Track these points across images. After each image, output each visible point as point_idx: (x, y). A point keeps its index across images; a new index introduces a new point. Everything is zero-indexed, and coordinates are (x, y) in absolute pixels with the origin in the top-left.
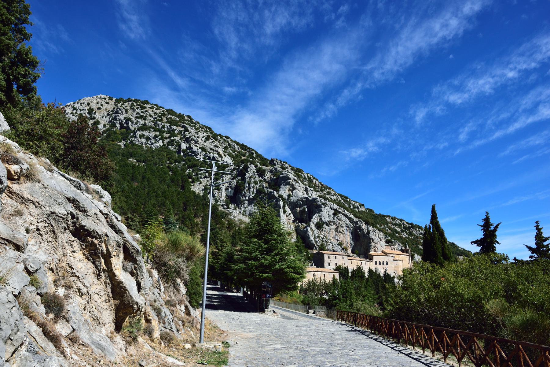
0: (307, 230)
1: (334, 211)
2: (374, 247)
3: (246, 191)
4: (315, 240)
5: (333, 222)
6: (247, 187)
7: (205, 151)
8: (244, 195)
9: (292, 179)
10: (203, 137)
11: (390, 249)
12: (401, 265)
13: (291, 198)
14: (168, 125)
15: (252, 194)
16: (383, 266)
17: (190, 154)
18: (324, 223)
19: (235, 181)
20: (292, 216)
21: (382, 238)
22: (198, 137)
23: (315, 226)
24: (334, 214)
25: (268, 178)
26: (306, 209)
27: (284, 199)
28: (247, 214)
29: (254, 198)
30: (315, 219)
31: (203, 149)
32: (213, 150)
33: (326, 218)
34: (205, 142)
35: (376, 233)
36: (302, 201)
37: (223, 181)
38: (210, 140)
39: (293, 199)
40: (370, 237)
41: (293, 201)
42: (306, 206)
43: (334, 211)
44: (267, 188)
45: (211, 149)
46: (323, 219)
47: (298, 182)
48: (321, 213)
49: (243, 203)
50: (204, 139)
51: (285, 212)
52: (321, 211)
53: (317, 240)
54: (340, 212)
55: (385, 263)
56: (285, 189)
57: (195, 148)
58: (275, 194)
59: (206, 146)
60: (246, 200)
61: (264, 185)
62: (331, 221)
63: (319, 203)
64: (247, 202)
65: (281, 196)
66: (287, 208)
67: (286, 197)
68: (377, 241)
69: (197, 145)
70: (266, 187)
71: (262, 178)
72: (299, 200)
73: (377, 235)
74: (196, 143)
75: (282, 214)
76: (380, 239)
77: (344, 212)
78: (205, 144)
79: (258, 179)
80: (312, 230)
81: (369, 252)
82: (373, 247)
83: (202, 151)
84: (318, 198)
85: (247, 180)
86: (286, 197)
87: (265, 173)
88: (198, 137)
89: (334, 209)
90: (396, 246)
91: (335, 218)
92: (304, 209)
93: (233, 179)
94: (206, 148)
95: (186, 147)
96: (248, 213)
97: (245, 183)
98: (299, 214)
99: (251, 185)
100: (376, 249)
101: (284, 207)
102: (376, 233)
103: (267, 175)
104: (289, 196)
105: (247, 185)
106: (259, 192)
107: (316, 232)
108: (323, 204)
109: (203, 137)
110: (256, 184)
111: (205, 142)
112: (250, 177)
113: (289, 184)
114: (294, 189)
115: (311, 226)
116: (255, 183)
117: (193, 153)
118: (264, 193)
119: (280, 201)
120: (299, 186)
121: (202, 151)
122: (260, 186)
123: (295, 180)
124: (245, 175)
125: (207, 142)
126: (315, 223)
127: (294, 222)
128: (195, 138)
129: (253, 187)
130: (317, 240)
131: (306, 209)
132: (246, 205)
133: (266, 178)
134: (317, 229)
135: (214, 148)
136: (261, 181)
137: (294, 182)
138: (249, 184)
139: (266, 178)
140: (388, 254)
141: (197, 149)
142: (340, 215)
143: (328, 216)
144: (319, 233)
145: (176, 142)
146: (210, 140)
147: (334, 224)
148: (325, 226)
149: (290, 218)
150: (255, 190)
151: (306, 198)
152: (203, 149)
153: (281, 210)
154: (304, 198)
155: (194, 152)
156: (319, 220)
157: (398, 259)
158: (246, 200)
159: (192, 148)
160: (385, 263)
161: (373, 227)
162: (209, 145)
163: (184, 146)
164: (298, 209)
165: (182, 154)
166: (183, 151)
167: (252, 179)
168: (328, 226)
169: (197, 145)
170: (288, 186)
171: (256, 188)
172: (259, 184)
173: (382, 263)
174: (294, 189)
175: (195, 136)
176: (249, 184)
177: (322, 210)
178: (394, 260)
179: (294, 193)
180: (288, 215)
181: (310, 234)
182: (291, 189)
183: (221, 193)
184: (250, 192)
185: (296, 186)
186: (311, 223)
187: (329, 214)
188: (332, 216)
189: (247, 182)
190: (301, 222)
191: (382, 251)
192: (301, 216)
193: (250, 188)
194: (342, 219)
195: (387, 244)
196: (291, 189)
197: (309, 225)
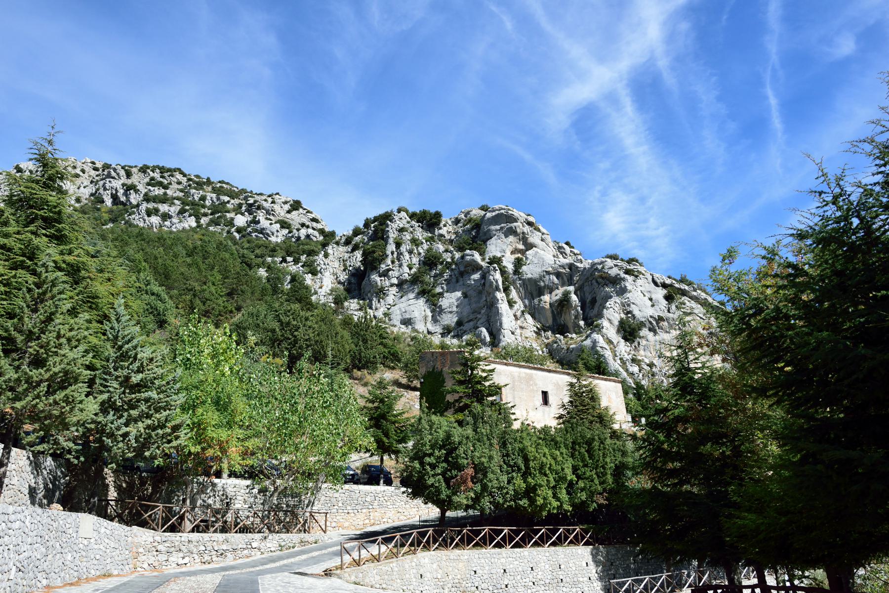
0: (595, 342)
1: (665, 292)
3: (389, 262)
4: (627, 371)
5: (667, 320)
6: (392, 253)
7: (288, 228)
8: (385, 274)
9: (522, 220)
10: (285, 203)
13: (524, 268)
14: (214, 196)
15: (406, 270)
17: (253, 235)
18: (642, 325)
19: (358, 255)
20: (528, 317)
22: (273, 202)
23: (618, 331)
24: (669, 298)
25: (449, 232)
26: (574, 298)
27: (503, 272)
28: (398, 323)
29: (415, 280)
30: (613, 313)
31: (284, 224)
32: (308, 227)
33: (643, 310)
34: (289, 212)
36: (558, 275)
37: (326, 255)
38: (301, 210)
39: (530, 271)
41: (529, 276)
42: (571, 288)
43: (665, 292)
44: (451, 252)
45: (303, 225)
46: (636, 312)
47: (539, 230)
48: (628, 295)
49: (381, 293)
50: (287, 207)
51: (511, 303)
52: (623, 291)
53: (635, 369)
54: (684, 293)
56: (504, 247)
57: (264, 223)
58: (477, 257)
59: (292, 220)
60: (392, 285)
61: (441, 247)
62: (661, 319)
63: (614, 272)
64: (394, 290)
65: (496, 261)
66: (514, 294)
67: (508, 263)
69: (271, 217)
70: (446, 251)
71: (433, 232)
72: (548, 273)
74: (268, 212)
75: (503, 307)
77: (695, 293)
78: (288, 216)
79: (420, 234)
80: (610, 342)
83: (282, 227)
84: (608, 260)
85: (392, 235)
86: (508, 263)
87: (440, 221)
88: (273, 202)
89: (664, 286)
91: (673, 307)
92: (566, 295)
93: (353, 250)
94: (291, 222)
95: (247, 222)
96: (399, 317)
97: (386, 243)
98: (549, 315)
99: (403, 248)
101: (506, 290)
103: (445, 226)
104: (518, 264)
105: (391, 247)
106: (430, 261)
107: (623, 348)
108: (628, 272)
109: (285, 203)
110: (417, 245)
111: (289, 212)
112: (401, 230)
113: (512, 232)
114: (529, 246)
115: (604, 330)
116: (415, 242)
117: (261, 233)
118: (442, 263)
119: (495, 270)
120: (542, 240)
121: (282, 227)
122: (429, 250)
123: (530, 224)
124: (387, 226)
125: (294, 213)
126: (616, 323)
127: (538, 333)
128: (265, 204)
129: (410, 252)
130: (635, 369)
131: (574, 298)
132: (390, 299)
133: (443, 231)
134: (626, 339)
135: (307, 223)
136: (431, 240)
137: (527, 229)
138: (398, 245)
139: (443, 231)
141: (271, 224)
142: (685, 299)
143: (650, 303)
144: (633, 352)
145: (226, 220)
146: (301, 210)
147: (671, 327)
148: (644, 332)
149: (525, 325)
150: (415, 260)
151: (571, 266)
152: (284, 224)
153: (500, 295)
154: (563, 267)
155: (262, 231)
156: (623, 316)
158: (392, 285)
159: (258, 222)
162: (296, 218)
163: (241, 221)
164: (546, 298)
165: (237, 236)
166: (239, 231)
167: (405, 233)
168: (655, 333)
169: (271, 217)
170: (511, 238)
171: (419, 254)
172: (425, 246)
174: (529, 246)
175: (266, 200)
176: (398, 245)
177: (629, 287)
179: (530, 257)
180: (519, 314)
181: (608, 354)
182: (521, 246)
183: (321, 279)
184: (400, 266)
185: (534, 238)
186: (605, 323)
187: (651, 299)
188: (664, 302)
189: (391, 241)
190: (562, 330)
192: (554, 319)
193: (400, 254)
194: (696, 311)
196: (521, 246)
197: (598, 329)
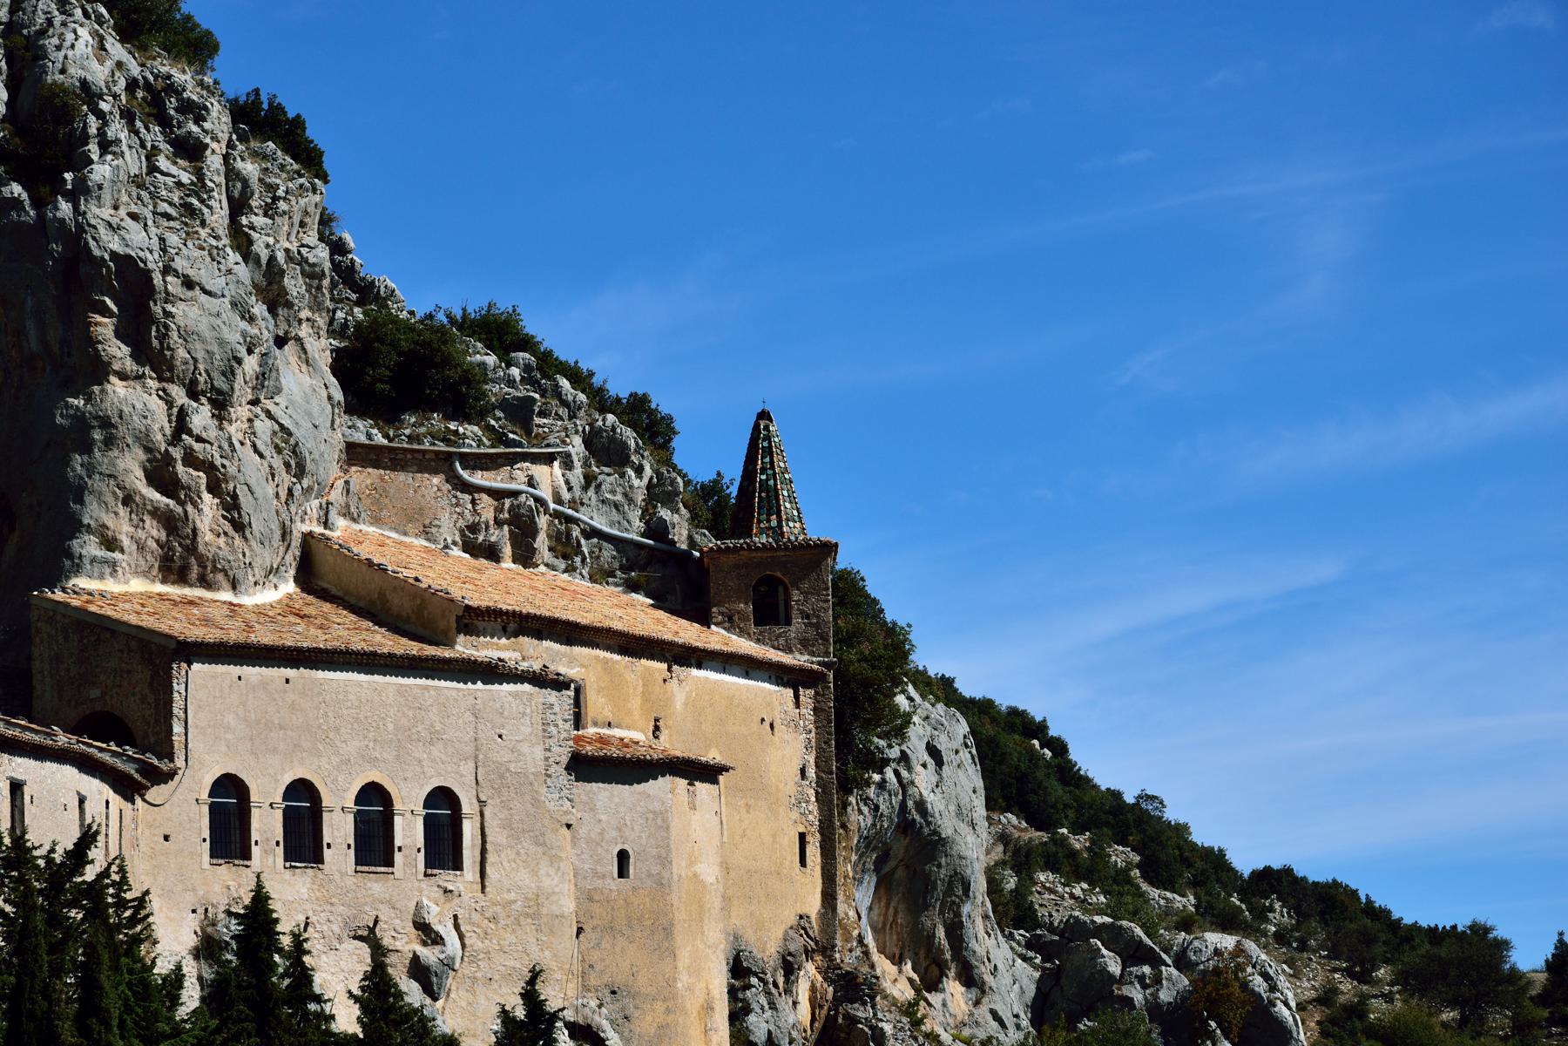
2: (160, 475)
11: (448, 530)
12: (709, 872)
16: (376, 886)
21: (294, 285)
35: (190, 151)
40: (76, 236)
55: (409, 831)
68: (234, 331)
73: (219, 215)
76: (276, 300)
81: (61, 564)
82: (131, 466)
90: (549, 478)
100: (207, 515)
102: (190, 151)
140: (475, 620)
157: (633, 735)
160: (409, 831)
161: (126, 35)
173: (339, 829)
178: (586, 767)
191: (308, 576)
195: (364, 431)
